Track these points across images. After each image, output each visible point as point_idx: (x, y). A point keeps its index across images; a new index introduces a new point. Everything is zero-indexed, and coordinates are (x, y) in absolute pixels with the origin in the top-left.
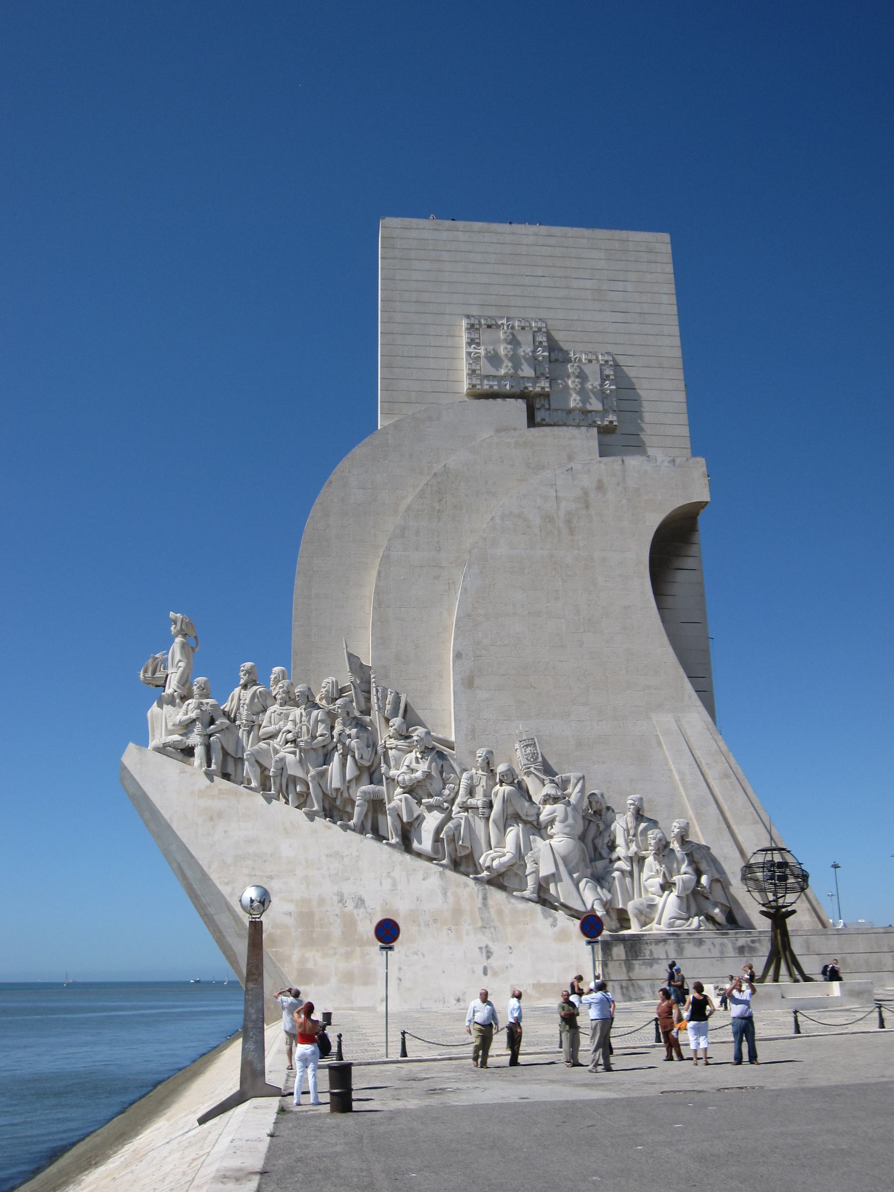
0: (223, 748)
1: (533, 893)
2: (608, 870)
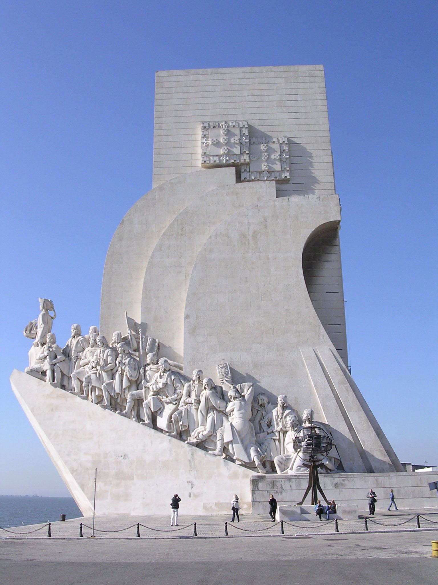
0: (61, 371)
2: (266, 438)
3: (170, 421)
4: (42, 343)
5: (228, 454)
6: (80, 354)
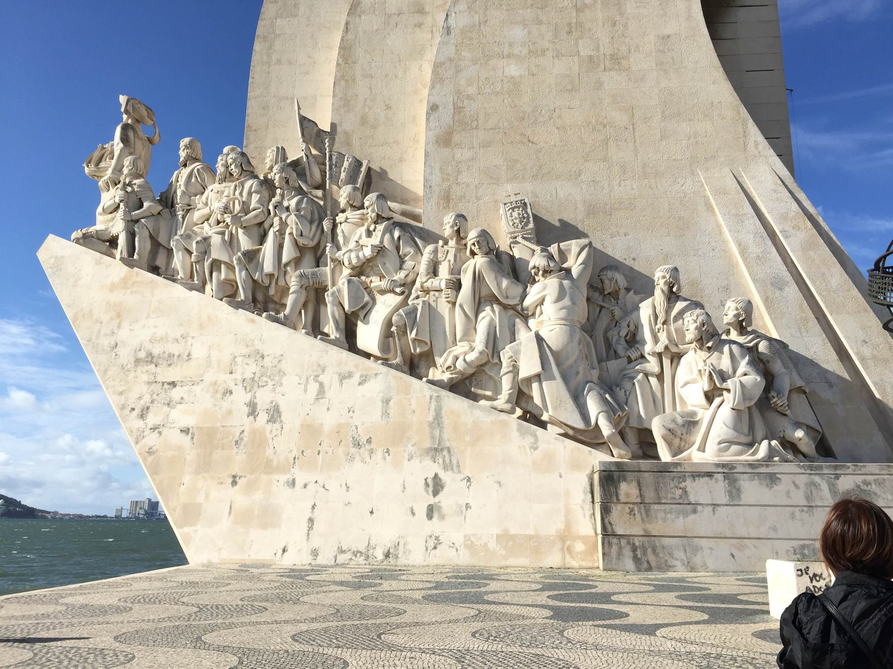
0: (151, 237)
1: (508, 402)
3: (387, 334)
5: (529, 408)
6: (195, 200)
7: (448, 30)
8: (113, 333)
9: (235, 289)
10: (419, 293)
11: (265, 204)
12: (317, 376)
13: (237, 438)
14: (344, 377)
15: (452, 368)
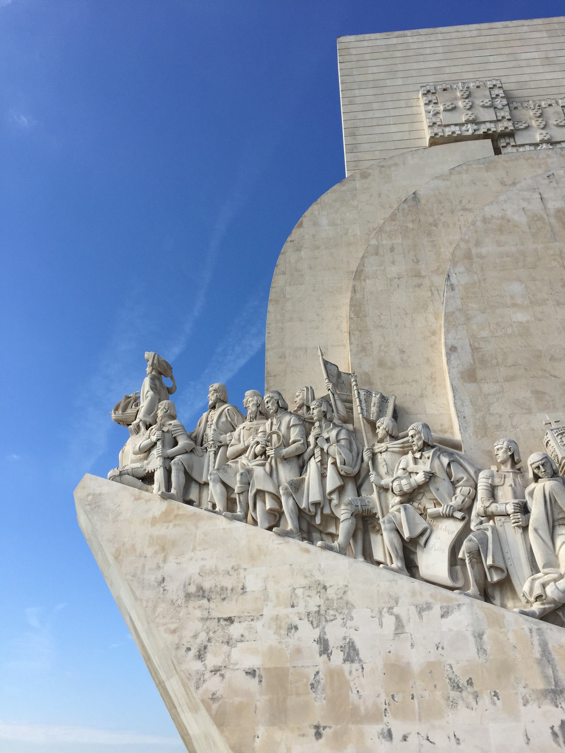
0: (186, 473)
4: (148, 423)
7: (452, 288)
8: (159, 567)
9: (277, 520)
10: (483, 519)
11: (305, 437)
12: (391, 608)
13: (311, 680)
14: (423, 609)
15: (544, 597)
